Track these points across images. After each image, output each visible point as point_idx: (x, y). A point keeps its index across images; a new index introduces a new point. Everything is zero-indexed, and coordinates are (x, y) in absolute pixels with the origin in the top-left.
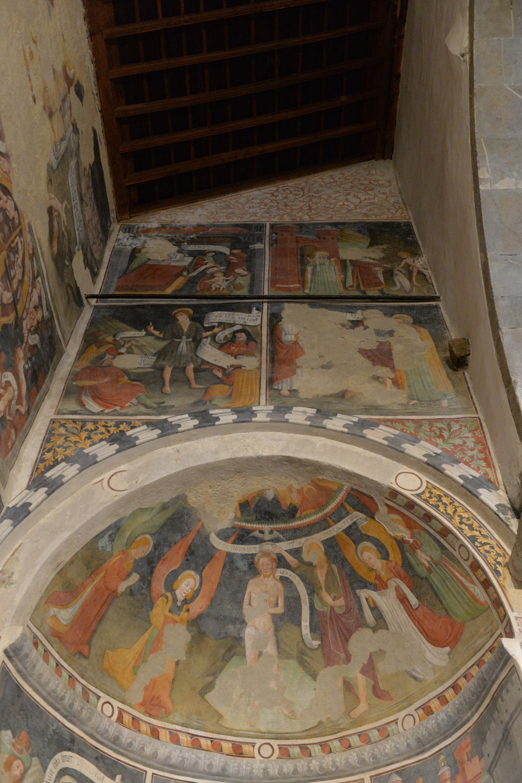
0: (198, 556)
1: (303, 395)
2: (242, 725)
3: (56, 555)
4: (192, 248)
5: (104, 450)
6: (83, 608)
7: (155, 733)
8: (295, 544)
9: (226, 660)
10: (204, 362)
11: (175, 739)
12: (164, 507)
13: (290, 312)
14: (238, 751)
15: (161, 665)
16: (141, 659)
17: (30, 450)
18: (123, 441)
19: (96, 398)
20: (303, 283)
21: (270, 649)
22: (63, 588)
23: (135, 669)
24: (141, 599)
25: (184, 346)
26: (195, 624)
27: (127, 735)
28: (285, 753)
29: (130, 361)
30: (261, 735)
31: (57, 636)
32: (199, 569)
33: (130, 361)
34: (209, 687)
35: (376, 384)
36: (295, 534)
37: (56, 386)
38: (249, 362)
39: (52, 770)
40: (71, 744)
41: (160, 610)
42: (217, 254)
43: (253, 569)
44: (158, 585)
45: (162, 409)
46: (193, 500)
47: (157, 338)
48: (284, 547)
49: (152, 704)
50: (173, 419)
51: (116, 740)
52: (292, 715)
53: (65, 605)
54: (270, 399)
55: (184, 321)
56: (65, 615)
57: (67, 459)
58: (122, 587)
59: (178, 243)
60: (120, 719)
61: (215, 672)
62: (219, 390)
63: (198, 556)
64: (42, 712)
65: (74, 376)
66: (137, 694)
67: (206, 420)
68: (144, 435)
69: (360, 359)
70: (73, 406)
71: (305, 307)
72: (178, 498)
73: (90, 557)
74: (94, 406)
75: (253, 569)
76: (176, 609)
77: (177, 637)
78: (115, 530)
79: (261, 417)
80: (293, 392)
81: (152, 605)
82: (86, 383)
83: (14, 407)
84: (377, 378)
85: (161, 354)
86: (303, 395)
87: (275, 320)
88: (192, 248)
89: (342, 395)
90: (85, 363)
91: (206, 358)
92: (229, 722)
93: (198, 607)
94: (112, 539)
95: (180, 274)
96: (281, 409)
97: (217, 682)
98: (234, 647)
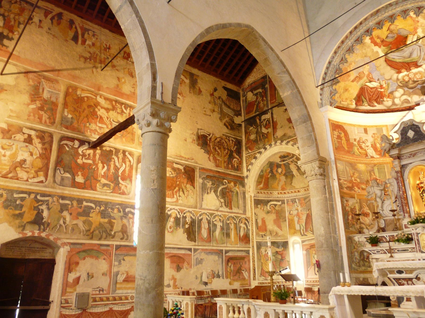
0: (278, 166)
1: (279, 137)
2: (298, 187)
3: (255, 181)
4: (255, 92)
5: (253, 161)
6: (264, 183)
7: (285, 193)
8: (292, 159)
9: (292, 178)
10: (263, 133)
11: (288, 193)
12: (267, 164)
13: (275, 110)
14: (299, 191)
15: (282, 183)
16: (278, 183)
17: (245, 165)
18: (255, 158)
19: (250, 149)
20: (275, 99)
21: (298, 174)
22: (259, 183)
23: (278, 186)
24: (273, 176)
25: (259, 129)
26: (285, 175)
27: (279, 196)
28: (305, 190)
29: (253, 137)
30: (302, 188)
31: (262, 189)
32: (280, 167)
33: (253, 137)
34: (292, 183)
35: (290, 129)
36: (291, 158)
37: (244, 148)
38: (270, 130)
39: (268, 206)
40: (271, 201)
41: (278, 176)
42: (260, 92)
43: (289, 164)
44: (275, 172)
45: (259, 148)
46: (271, 160)
47: (255, 128)
48: (291, 160)
49: (283, 189)
50: (261, 150)
51: (278, 197)
52: (305, 184)
53: (260, 184)
54: (274, 140)
55: (258, 121)
56: (262, 186)
57: (250, 165)
58: (269, 176)
59: (252, 92)
60: (278, 194)
61: (292, 180)
62: (266, 140)
63: (278, 166)
64: (264, 200)
65: (246, 144)
66: (280, 188)
67: (265, 149)
68: (258, 155)
69: (287, 122)
70: (247, 152)
71: (276, 108)
72: (269, 162)
73: (261, 176)
74: (250, 151)
75: (289, 164)
76: (280, 174)
77: (283, 178)
78: (262, 171)
79: (273, 145)
80: (277, 137)
81: (276, 176)
82: (248, 145)
83: (238, 162)
84: (290, 127)
85: (257, 133)
86: (279, 137)
87: (272, 114)
88: (255, 92)
89: (284, 135)
90: (246, 140)
91: (263, 131)
92: (296, 187)
93: (284, 172)
94: (262, 172)
95: (255, 104)
96: (276, 142)
97: (293, 182)
98: (293, 176)
